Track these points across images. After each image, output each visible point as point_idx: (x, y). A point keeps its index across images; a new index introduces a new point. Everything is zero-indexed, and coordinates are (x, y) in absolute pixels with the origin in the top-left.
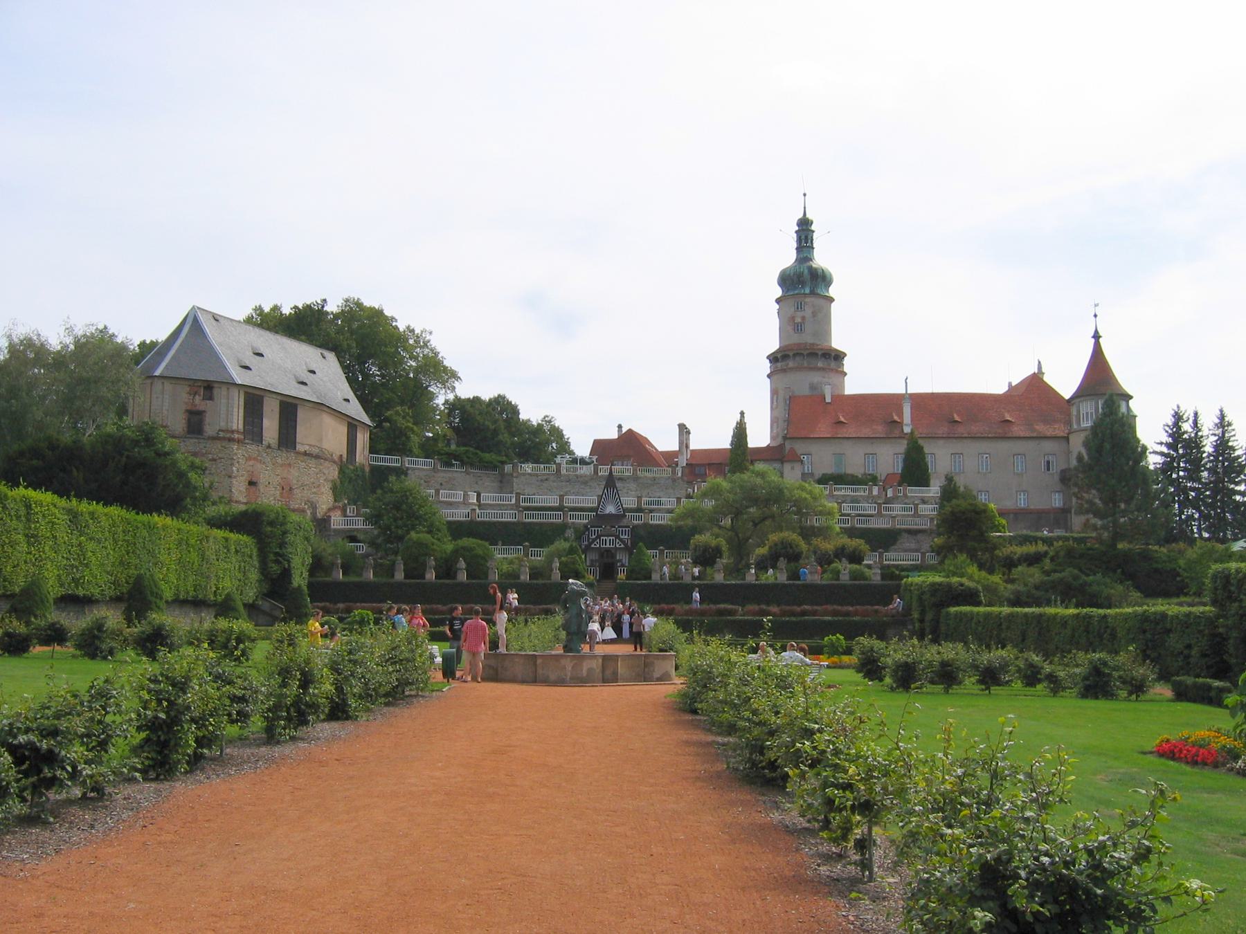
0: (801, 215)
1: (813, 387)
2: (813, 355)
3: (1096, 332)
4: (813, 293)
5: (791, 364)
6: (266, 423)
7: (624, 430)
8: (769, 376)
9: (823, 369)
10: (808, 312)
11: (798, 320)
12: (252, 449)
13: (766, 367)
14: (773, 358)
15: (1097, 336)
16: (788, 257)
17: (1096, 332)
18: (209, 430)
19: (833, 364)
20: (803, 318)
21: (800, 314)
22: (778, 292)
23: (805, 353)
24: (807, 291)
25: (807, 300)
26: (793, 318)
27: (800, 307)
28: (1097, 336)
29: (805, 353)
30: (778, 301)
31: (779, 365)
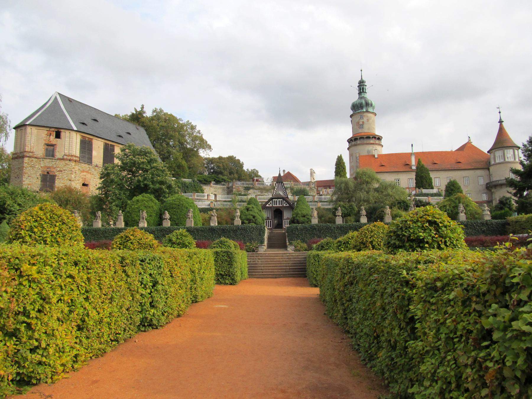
0: (360, 79)
1: (368, 151)
2: (368, 138)
3: (500, 119)
4: (367, 111)
5: (358, 142)
6: (94, 153)
7: (286, 172)
8: (348, 149)
9: (373, 144)
10: (365, 120)
11: (361, 123)
12: (85, 166)
13: (347, 145)
14: (350, 141)
15: (501, 122)
16: (355, 98)
17: (500, 119)
18: (58, 155)
19: (377, 142)
20: (363, 122)
21: (362, 120)
22: (351, 112)
24: (364, 110)
26: (358, 123)
27: (362, 118)
28: (501, 122)
30: (351, 116)
31: (353, 143)
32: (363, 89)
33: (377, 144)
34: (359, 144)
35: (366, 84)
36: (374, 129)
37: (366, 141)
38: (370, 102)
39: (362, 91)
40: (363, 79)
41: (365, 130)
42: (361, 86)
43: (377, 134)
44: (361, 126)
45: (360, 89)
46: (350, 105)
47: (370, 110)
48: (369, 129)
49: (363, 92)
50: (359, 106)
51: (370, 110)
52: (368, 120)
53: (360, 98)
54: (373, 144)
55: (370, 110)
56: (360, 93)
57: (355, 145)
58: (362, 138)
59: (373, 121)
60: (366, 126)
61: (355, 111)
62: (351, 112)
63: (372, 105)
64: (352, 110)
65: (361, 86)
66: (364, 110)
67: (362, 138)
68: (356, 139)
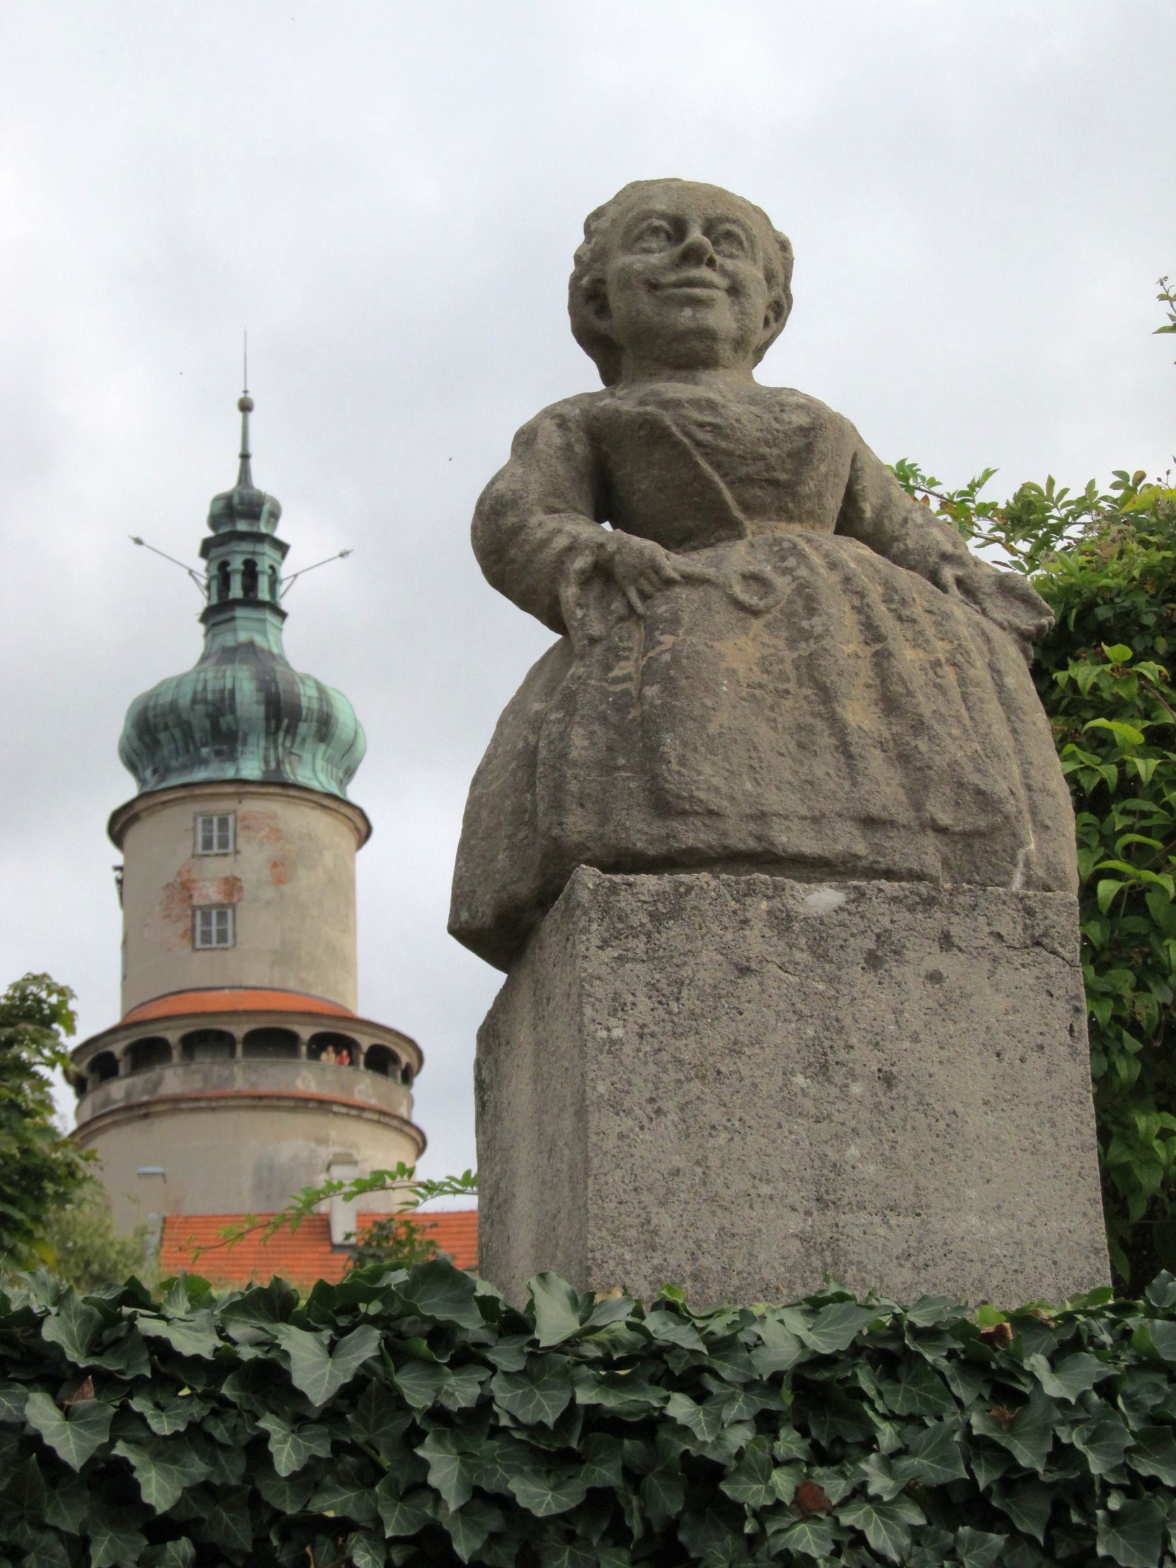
0: (228, 483)
2: (274, 1041)
4: (277, 783)
5: (173, 1079)
9: (322, 1105)
10: (251, 860)
11: (210, 893)
19: (366, 1087)
20: (232, 885)
21: (217, 867)
22: (126, 788)
23: (239, 1031)
25: (251, 806)
26: (184, 888)
27: (218, 839)
29: (239, 1031)
30: (121, 825)
31: (118, 1090)
32: (250, 572)
33: (357, 1111)
34: (176, 1104)
35: (281, 533)
36: (344, 961)
37: (243, 1074)
38: (307, 695)
39: (236, 591)
40: (262, 482)
41: (248, 973)
42: (240, 546)
43: (363, 1011)
44: (210, 922)
45: (222, 577)
46: (114, 726)
47: (310, 770)
48: (285, 956)
49: (250, 600)
50: (199, 721)
51: (310, 770)
52: (281, 871)
53: (222, 655)
54: (322, 1105)
55: (302, 774)
56: (216, 615)
57: (139, 1111)
58: (207, 1040)
59: (342, 887)
60: (256, 927)
61: (163, 771)
62: (126, 788)
63: (325, 726)
64: (132, 764)
65: (240, 546)
66: (251, 768)
67: (207, 1040)
68: (148, 1052)
